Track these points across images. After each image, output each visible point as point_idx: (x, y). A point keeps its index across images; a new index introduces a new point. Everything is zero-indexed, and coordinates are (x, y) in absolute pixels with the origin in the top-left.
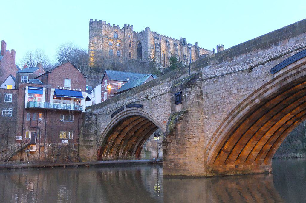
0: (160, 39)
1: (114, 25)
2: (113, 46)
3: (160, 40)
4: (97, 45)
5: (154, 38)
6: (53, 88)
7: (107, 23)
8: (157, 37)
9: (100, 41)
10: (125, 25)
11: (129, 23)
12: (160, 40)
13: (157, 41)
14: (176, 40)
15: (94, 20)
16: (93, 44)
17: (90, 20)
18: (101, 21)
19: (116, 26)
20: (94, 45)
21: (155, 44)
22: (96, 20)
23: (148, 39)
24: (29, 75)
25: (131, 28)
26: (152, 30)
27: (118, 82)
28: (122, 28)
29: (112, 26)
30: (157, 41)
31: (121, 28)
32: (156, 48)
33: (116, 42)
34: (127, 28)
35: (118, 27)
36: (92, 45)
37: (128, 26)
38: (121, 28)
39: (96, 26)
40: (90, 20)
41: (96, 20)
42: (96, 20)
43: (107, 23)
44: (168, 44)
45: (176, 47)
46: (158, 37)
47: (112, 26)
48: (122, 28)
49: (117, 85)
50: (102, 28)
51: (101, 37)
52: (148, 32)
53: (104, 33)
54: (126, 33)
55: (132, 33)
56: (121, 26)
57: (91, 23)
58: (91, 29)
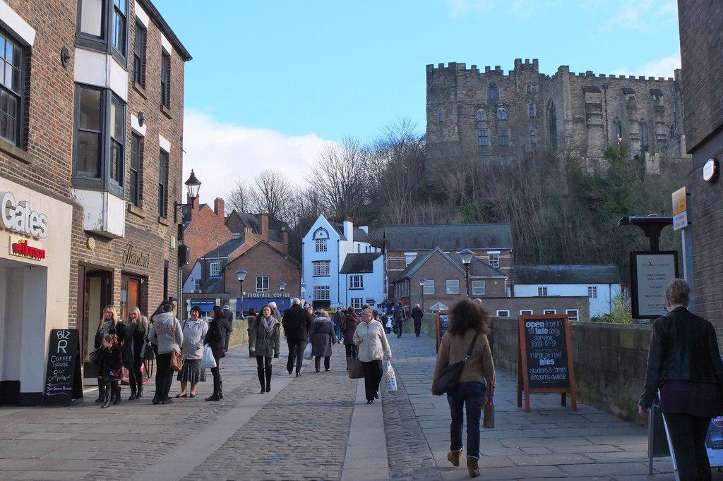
0: (605, 87)
1: (487, 68)
2: (488, 122)
3: (603, 91)
4: (446, 126)
5: (585, 90)
6: (233, 297)
7: (468, 67)
8: (591, 83)
9: (454, 116)
10: (517, 61)
11: (526, 56)
12: (603, 91)
13: (591, 98)
14: (661, 80)
15: (436, 67)
16: (435, 124)
17: (428, 66)
18: (452, 65)
19: (493, 68)
20: (439, 127)
21: (587, 106)
22: (441, 65)
23: (565, 97)
24: (221, 261)
25: (531, 69)
26: (576, 69)
27: (406, 254)
28: (510, 72)
29: (482, 71)
30: (591, 98)
31: (506, 73)
32: (588, 116)
33: (495, 111)
34: (526, 69)
35: (498, 71)
36: (434, 128)
37: (523, 62)
38: (506, 73)
39: (441, 79)
40: (428, 66)
41: (440, 65)
42: (440, 65)
43: (468, 67)
44: (627, 98)
45: (658, 99)
46: (595, 85)
47: (482, 71)
48: (510, 72)
49: (405, 261)
50: (456, 83)
51: (455, 106)
52: (565, 79)
53: (461, 93)
54: (518, 83)
55: (536, 80)
56: (508, 68)
57: (431, 72)
58: (431, 91)
